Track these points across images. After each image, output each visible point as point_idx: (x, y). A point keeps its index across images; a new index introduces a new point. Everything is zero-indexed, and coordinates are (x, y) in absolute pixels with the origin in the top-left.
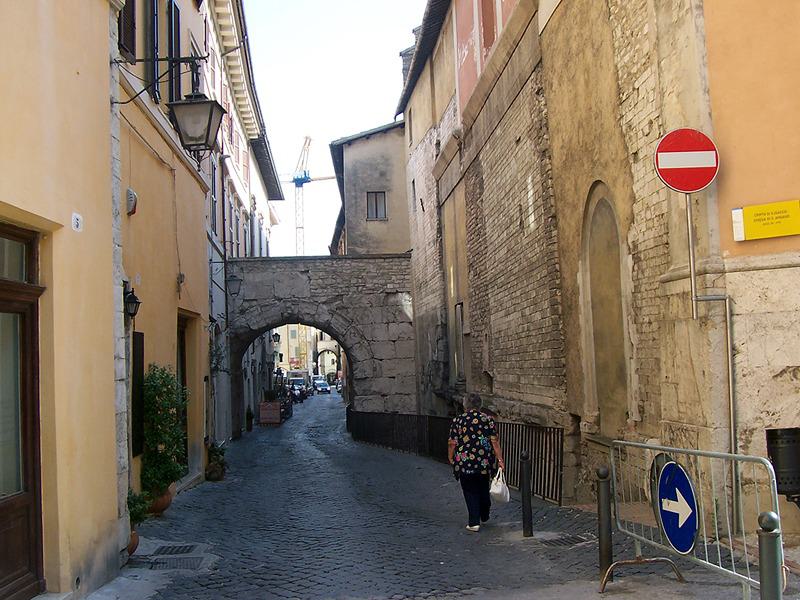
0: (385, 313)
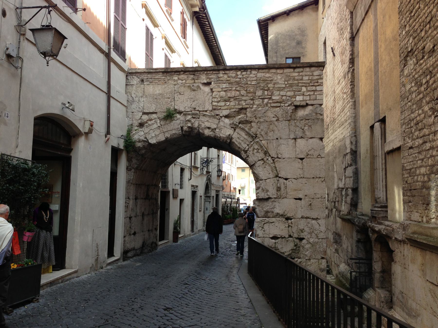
0: (292, 128)
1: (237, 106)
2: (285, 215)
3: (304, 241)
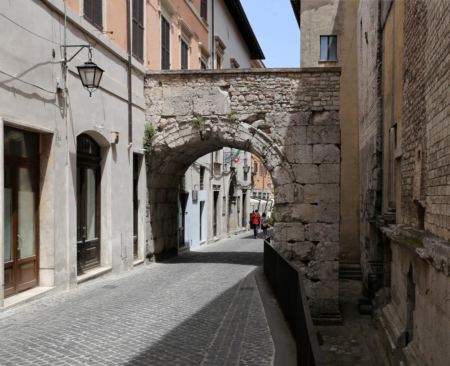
0: (309, 133)
1: (255, 111)
2: (301, 220)
3: (319, 244)
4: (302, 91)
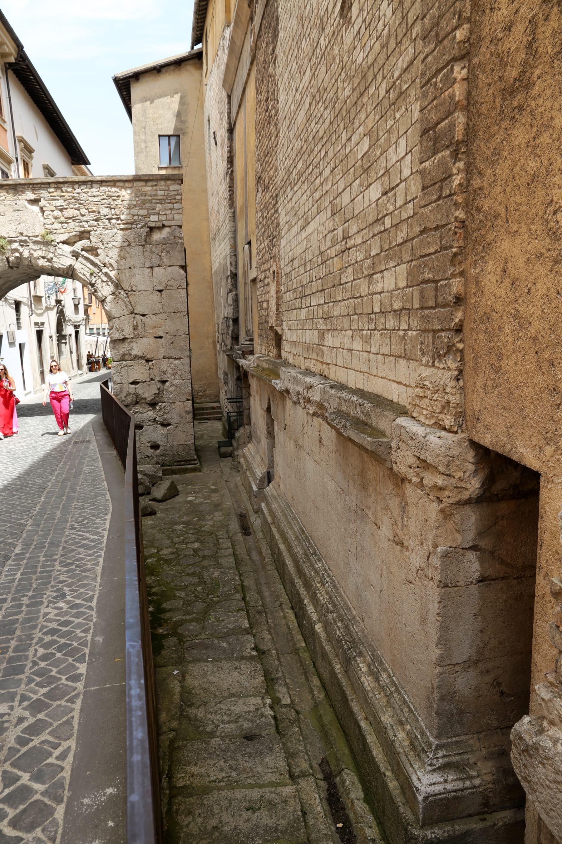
0: (147, 254)
4: (135, 203)
